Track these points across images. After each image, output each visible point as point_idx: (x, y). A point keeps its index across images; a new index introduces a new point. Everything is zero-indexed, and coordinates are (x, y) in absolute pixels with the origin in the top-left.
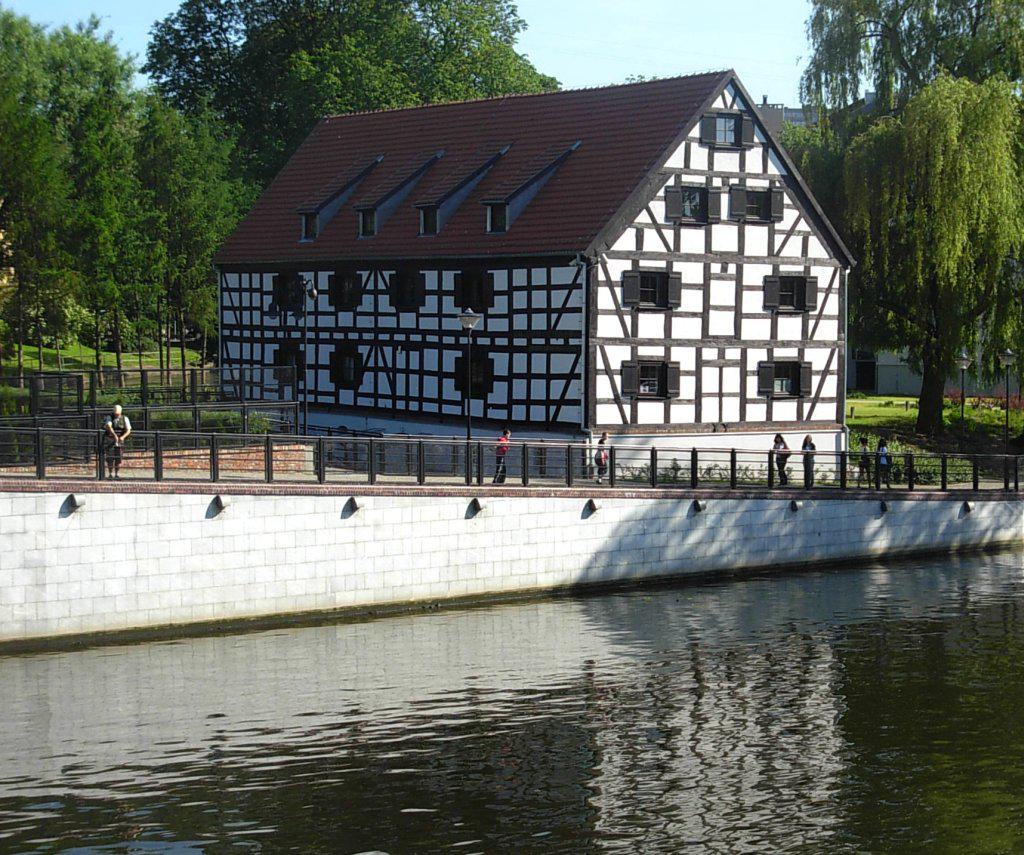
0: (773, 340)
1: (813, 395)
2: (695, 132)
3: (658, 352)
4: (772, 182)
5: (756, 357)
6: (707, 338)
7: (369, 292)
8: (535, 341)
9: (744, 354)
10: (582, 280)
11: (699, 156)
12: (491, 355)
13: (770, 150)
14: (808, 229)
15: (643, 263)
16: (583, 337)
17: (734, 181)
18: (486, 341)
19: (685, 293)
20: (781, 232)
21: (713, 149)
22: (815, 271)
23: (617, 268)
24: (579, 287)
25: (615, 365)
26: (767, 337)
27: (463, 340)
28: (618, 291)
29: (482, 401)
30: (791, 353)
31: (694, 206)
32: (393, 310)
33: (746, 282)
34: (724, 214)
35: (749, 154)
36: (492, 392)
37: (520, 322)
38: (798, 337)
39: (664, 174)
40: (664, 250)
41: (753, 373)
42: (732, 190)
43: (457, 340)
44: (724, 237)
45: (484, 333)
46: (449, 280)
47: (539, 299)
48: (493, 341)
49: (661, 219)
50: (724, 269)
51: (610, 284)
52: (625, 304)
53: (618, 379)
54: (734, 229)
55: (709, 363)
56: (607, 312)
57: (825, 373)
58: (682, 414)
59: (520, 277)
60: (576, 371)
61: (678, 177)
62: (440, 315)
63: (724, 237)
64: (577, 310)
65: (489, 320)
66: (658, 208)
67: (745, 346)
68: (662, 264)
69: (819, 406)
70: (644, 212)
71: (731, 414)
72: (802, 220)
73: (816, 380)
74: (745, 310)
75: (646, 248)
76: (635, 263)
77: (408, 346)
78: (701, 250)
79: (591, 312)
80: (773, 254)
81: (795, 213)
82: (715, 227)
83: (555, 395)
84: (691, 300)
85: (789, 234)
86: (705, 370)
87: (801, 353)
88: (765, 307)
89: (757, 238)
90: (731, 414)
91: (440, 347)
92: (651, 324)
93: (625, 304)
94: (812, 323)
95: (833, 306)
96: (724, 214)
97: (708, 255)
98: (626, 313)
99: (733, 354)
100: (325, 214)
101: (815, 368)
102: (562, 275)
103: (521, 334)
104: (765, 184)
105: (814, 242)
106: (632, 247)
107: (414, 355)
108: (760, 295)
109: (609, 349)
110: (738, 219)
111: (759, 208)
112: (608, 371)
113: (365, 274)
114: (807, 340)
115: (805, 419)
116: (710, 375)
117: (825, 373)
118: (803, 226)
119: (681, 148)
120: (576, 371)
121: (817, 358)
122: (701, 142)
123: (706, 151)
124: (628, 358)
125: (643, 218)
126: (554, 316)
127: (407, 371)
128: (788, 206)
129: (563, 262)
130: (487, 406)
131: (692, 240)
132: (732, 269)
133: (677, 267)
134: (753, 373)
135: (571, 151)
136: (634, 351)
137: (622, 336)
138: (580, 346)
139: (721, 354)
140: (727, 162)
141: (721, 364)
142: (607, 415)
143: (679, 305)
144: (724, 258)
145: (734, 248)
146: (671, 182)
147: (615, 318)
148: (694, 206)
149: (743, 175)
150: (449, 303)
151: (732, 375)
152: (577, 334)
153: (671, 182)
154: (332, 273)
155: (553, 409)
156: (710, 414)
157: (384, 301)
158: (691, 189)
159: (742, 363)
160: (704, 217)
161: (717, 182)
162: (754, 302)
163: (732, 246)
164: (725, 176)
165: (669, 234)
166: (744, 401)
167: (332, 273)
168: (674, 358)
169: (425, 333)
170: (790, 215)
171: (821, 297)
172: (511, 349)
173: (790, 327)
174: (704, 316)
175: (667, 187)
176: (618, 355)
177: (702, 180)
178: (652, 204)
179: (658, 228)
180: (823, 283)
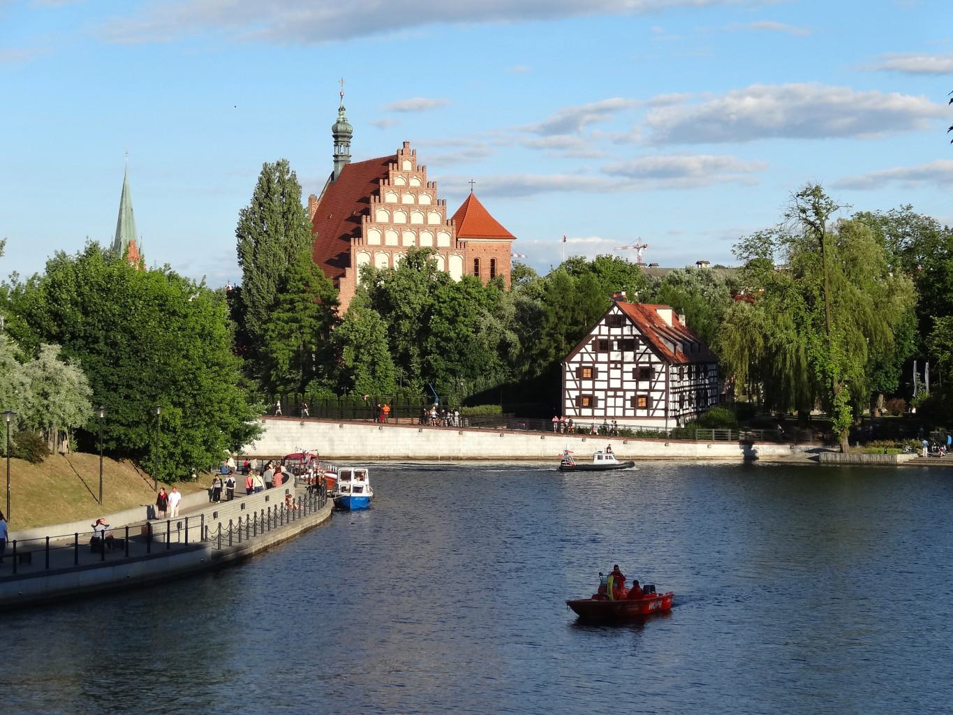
1: (654, 407)
2: (603, 322)
3: (591, 393)
5: (629, 395)
6: (610, 389)
9: (625, 394)
11: (605, 330)
13: (634, 328)
15: (583, 365)
17: (620, 337)
19: (599, 374)
22: (654, 366)
23: (573, 367)
26: (635, 388)
28: (574, 374)
30: (646, 393)
31: (604, 346)
33: (624, 370)
34: (615, 348)
38: (648, 388)
42: (618, 340)
44: (615, 356)
50: (616, 366)
51: (570, 371)
52: (577, 377)
53: (574, 402)
57: (659, 401)
58: (597, 413)
63: (615, 356)
66: (589, 348)
67: (625, 391)
68: (591, 365)
69: (656, 411)
71: (619, 412)
72: (648, 349)
73: (655, 403)
74: (624, 379)
75: (584, 360)
78: (606, 360)
80: (636, 362)
81: (645, 347)
82: (611, 353)
85: (642, 354)
86: (608, 399)
87: (649, 393)
89: (629, 356)
90: (619, 412)
92: (587, 384)
93: (577, 377)
94: (653, 384)
95: (663, 377)
96: (615, 348)
97: (610, 362)
99: (620, 393)
104: (632, 338)
106: (579, 360)
108: (631, 374)
109: (570, 391)
111: (626, 345)
112: (570, 399)
114: (651, 389)
115: (651, 415)
116: (611, 402)
117: (659, 401)
118: (649, 351)
119: (598, 327)
121: (655, 395)
122: (605, 325)
125: (583, 350)
131: (603, 357)
133: (597, 365)
136: (580, 393)
139: (615, 393)
140: (616, 331)
141: (615, 396)
142: (569, 412)
146: (594, 339)
148: (604, 346)
149: (622, 335)
151: (620, 402)
153: (594, 339)
156: (610, 412)
158: (601, 341)
159: (624, 397)
161: (612, 338)
162: (628, 376)
163: (619, 358)
164: (615, 336)
165: (593, 356)
166: (624, 409)
170: (643, 348)
171: (656, 375)
173: (644, 385)
176: (574, 394)
177: (606, 337)
179: (589, 354)
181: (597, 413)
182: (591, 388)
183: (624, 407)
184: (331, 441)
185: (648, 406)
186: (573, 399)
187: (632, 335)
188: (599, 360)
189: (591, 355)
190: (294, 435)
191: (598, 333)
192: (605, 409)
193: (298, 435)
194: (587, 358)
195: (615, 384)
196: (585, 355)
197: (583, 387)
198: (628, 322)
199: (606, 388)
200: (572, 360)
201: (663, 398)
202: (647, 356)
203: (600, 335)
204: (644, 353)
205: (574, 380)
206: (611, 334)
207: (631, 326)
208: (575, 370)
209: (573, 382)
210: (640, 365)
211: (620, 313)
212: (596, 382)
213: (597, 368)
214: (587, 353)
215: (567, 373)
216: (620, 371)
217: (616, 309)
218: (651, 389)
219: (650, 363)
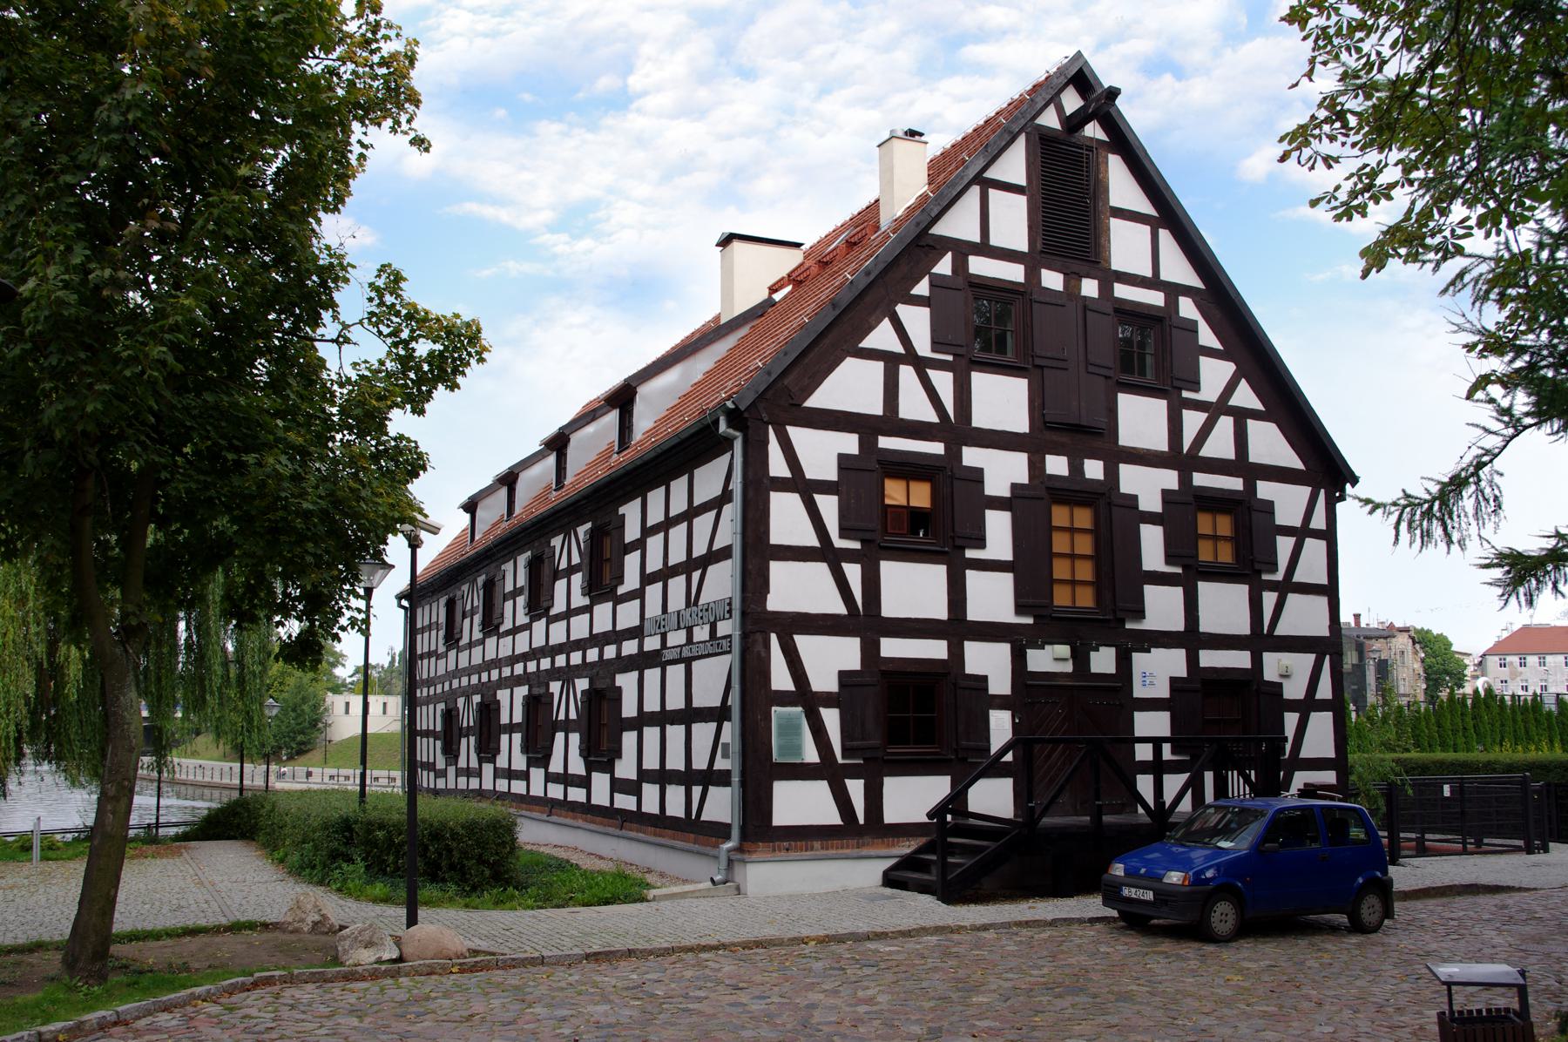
3: (936, 649)
15: (885, 442)
16: (736, 614)
25: (823, 680)
28: (828, 506)
29: (607, 776)
36: (620, 757)
39: (933, 248)
40: (931, 416)
51: (805, 488)
52: (841, 536)
53: (831, 718)
61: (960, 265)
64: (725, 553)
68: (937, 448)
70: (886, 325)
76: (867, 444)
93: (841, 536)
98: (850, 556)
112: (803, 695)
125: (882, 337)
130: (618, 786)
133: (972, 456)
136: (870, 650)
137: (838, 607)
143: (981, 543)
155: (697, 791)
172: (642, 661)
175: (937, 283)
178: (903, 310)
179: (921, 366)
182: (938, 609)
186: (828, 700)
188: (981, 418)
189: (935, 376)
200: (817, 400)
203: (984, 248)
205: (824, 552)
208: (831, 474)
209: (819, 572)
212: (971, 576)
213: (977, 475)
214: (911, 357)
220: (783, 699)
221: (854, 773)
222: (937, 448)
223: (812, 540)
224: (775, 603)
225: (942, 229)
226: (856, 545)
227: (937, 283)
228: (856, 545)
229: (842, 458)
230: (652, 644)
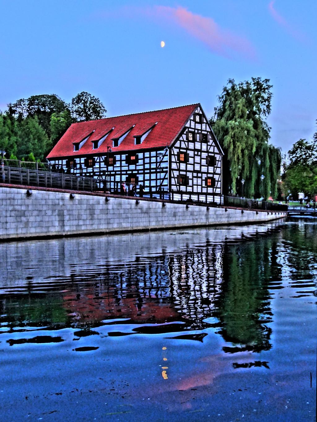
0: (208, 173)
2: (192, 118)
3: (184, 173)
4: (207, 133)
5: (204, 176)
6: (195, 171)
7: (98, 162)
8: (152, 171)
10: (168, 153)
11: (193, 123)
12: (137, 175)
14: (215, 145)
15: (181, 150)
17: (200, 131)
18: (136, 172)
20: (209, 145)
21: (196, 122)
22: (216, 156)
23: (176, 151)
24: (167, 155)
25: (176, 176)
26: (207, 172)
27: (129, 172)
30: (211, 176)
32: (106, 166)
34: (198, 140)
35: (203, 124)
37: (147, 166)
41: (204, 180)
43: (126, 172)
45: (135, 170)
46: (124, 157)
47: (153, 160)
48: (138, 172)
49: (185, 140)
50: (198, 153)
54: (200, 143)
55: (195, 177)
56: (174, 162)
57: (218, 181)
59: (147, 154)
60: (166, 177)
62: (121, 166)
64: (167, 161)
65: (137, 167)
66: (184, 136)
67: (202, 173)
68: (185, 151)
73: (216, 183)
76: (179, 150)
77: (111, 175)
79: (171, 162)
80: (207, 152)
82: (196, 142)
83: (159, 184)
84: (191, 160)
85: (211, 146)
88: (206, 164)
89: (204, 147)
91: (121, 175)
92: (183, 166)
94: (215, 168)
95: (219, 165)
96: (198, 140)
97: (195, 150)
99: (200, 175)
100: (81, 144)
101: (216, 180)
102: (163, 152)
103: (147, 169)
104: (206, 133)
105: (216, 148)
106: (179, 146)
107: (112, 178)
108: (205, 160)
110: (202, 141)
112: (174, 177)
113: (96, 158)
114: (214, 173)
117: (218, 181)
118: (214, 144)
120: (166, 177)
121: (216, 177)
122: (193, 120)
123: (194, 122)
124: (178, 174)
125: (181, 139)
126: (158, 164)
127: (110, 182)
128: (210, 139)
129: (162, 149)
131: (191, 146)
132: (199, 153)
133: (188, 152)
134: (204, 180)
135: (155, 125)
136: (179, 173)
138: (167, 171)
139: (197, 175)
140: (198, 126)
141: (197, 177)
143: (188, 162)
144: (198, 151)
145: (200, 149)
146: (187, 130)
147: (176, 164)
149: (201, 130)
150: (124, 163)
151: (199, 181)
152: (167, 168)
154: (86, 158)
157: (103, 164)
159: (201, 177)
160: (194, 141)
162: (204, 162)
164: (198, 130)
165: (186, 143)
166: (202, 187)
167: (86, 158)
168: (188, 175)
169: (116, 171)
171: (217, 162)
173: (211, 169)
174: (194, 165)
176: (176, 173)
177: (193, 130)
180: (218, 159)
181: (189, 189)
183: (201, 185)
184: (61, 215)
185: (213, 185)
187: (206, 131)
188: (189, 148)
190: (17, 207)
191: (189, 126)
192: (192, 187)
193: (23, 208)
194: (183, 145)
195: (197, 167)
196: (182, 142)
197: (181, 169)
198: (205, 121)
199: (192, 170)
201: (220, 180)
202: (213, 147)
204: (211, 146)
206: (196, 128)
207: (206, 123)
210: (210, 154)
211: (201, 113)
214: (183, 141)
215: (172, 156)
216: (200, 157)
217: (199, 108)
218: (214, 173)
219: (213, 153)
220: (173, 177)
221: (178, 185)
222: (185, 151)
223: (175, 161)
224: (172, 168)
225: (186, 126)
226: (178, 161)
227: (186, 132)
228: (178, 161)
229: (177, 152)
230: (146, 171)
